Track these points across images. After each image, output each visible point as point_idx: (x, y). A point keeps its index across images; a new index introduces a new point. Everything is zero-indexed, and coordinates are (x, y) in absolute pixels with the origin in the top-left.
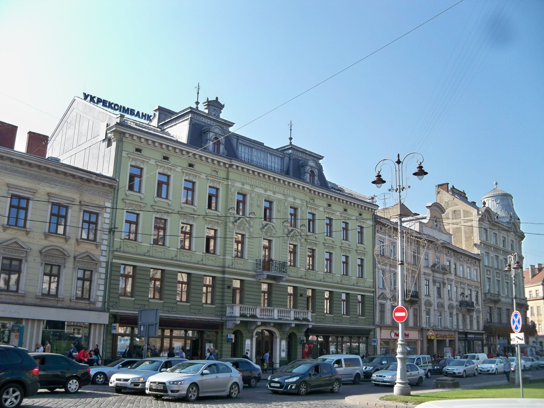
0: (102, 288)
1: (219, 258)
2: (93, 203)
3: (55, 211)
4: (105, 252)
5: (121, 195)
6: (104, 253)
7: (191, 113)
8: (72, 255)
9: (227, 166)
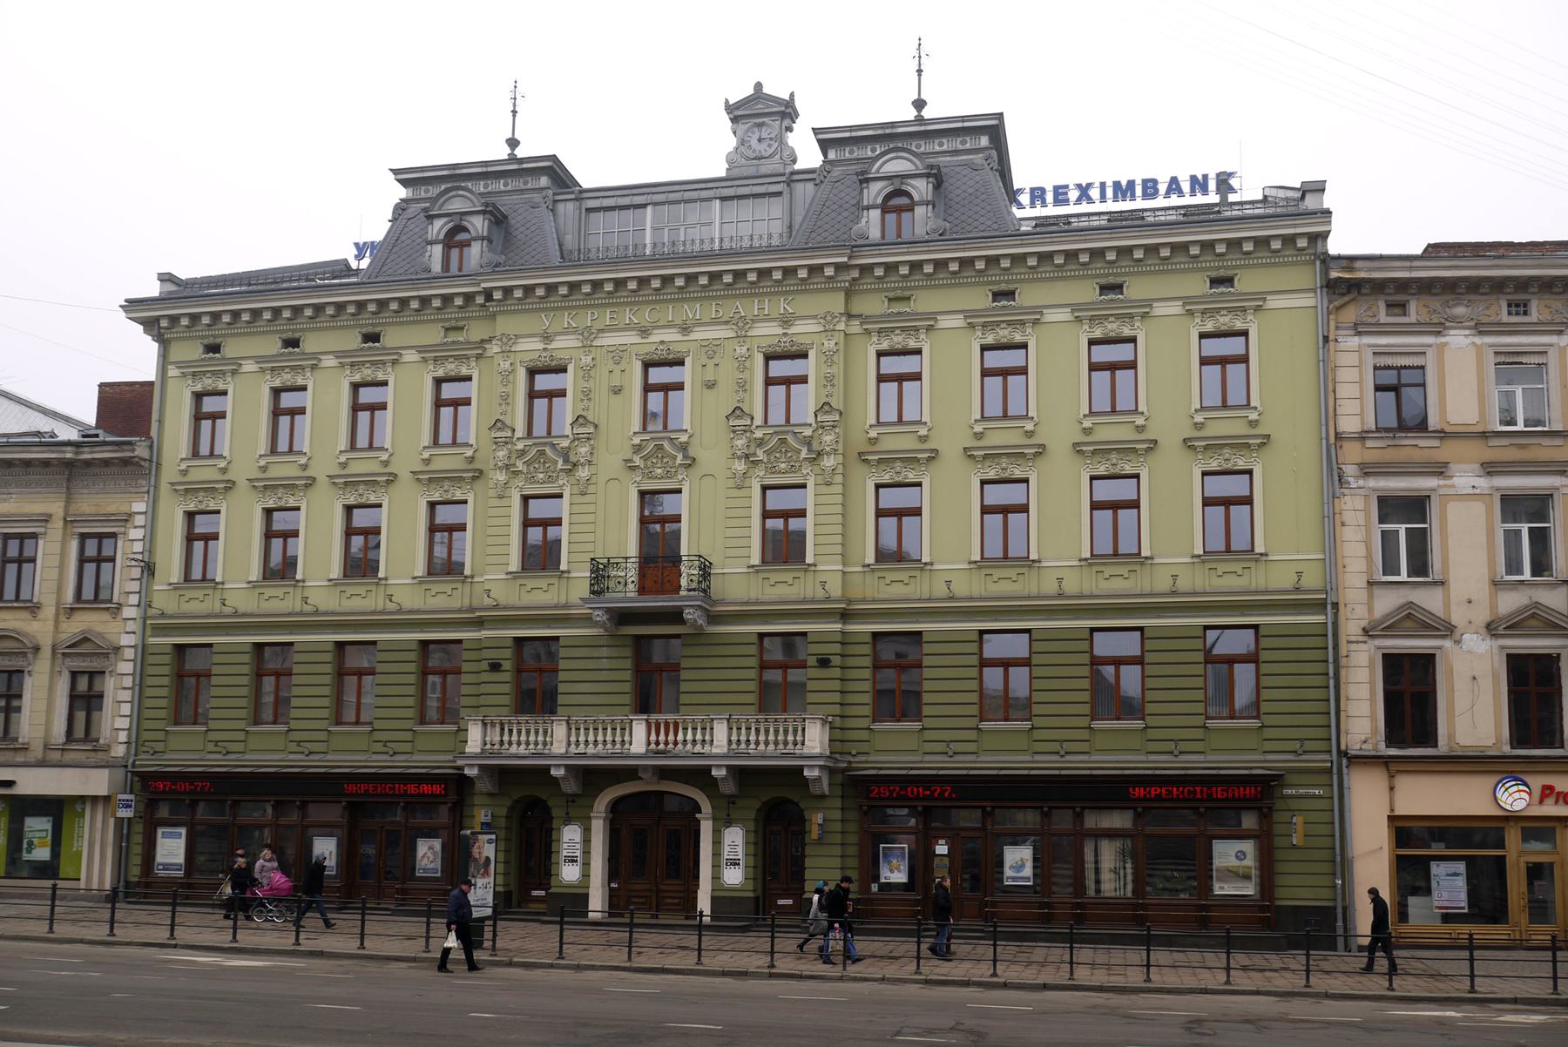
0: (126, 709)
1: (40, 593)
2: (104, 512)
3: (91, 550)
4: (131, 622)
5: (169, 473)
6: (131, 626)
7: (548, 175)
8: (46, 642)
9: (480, 300)
